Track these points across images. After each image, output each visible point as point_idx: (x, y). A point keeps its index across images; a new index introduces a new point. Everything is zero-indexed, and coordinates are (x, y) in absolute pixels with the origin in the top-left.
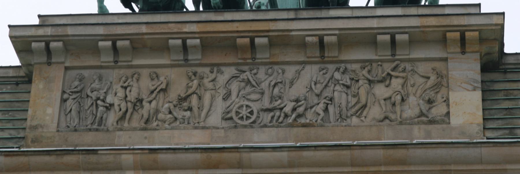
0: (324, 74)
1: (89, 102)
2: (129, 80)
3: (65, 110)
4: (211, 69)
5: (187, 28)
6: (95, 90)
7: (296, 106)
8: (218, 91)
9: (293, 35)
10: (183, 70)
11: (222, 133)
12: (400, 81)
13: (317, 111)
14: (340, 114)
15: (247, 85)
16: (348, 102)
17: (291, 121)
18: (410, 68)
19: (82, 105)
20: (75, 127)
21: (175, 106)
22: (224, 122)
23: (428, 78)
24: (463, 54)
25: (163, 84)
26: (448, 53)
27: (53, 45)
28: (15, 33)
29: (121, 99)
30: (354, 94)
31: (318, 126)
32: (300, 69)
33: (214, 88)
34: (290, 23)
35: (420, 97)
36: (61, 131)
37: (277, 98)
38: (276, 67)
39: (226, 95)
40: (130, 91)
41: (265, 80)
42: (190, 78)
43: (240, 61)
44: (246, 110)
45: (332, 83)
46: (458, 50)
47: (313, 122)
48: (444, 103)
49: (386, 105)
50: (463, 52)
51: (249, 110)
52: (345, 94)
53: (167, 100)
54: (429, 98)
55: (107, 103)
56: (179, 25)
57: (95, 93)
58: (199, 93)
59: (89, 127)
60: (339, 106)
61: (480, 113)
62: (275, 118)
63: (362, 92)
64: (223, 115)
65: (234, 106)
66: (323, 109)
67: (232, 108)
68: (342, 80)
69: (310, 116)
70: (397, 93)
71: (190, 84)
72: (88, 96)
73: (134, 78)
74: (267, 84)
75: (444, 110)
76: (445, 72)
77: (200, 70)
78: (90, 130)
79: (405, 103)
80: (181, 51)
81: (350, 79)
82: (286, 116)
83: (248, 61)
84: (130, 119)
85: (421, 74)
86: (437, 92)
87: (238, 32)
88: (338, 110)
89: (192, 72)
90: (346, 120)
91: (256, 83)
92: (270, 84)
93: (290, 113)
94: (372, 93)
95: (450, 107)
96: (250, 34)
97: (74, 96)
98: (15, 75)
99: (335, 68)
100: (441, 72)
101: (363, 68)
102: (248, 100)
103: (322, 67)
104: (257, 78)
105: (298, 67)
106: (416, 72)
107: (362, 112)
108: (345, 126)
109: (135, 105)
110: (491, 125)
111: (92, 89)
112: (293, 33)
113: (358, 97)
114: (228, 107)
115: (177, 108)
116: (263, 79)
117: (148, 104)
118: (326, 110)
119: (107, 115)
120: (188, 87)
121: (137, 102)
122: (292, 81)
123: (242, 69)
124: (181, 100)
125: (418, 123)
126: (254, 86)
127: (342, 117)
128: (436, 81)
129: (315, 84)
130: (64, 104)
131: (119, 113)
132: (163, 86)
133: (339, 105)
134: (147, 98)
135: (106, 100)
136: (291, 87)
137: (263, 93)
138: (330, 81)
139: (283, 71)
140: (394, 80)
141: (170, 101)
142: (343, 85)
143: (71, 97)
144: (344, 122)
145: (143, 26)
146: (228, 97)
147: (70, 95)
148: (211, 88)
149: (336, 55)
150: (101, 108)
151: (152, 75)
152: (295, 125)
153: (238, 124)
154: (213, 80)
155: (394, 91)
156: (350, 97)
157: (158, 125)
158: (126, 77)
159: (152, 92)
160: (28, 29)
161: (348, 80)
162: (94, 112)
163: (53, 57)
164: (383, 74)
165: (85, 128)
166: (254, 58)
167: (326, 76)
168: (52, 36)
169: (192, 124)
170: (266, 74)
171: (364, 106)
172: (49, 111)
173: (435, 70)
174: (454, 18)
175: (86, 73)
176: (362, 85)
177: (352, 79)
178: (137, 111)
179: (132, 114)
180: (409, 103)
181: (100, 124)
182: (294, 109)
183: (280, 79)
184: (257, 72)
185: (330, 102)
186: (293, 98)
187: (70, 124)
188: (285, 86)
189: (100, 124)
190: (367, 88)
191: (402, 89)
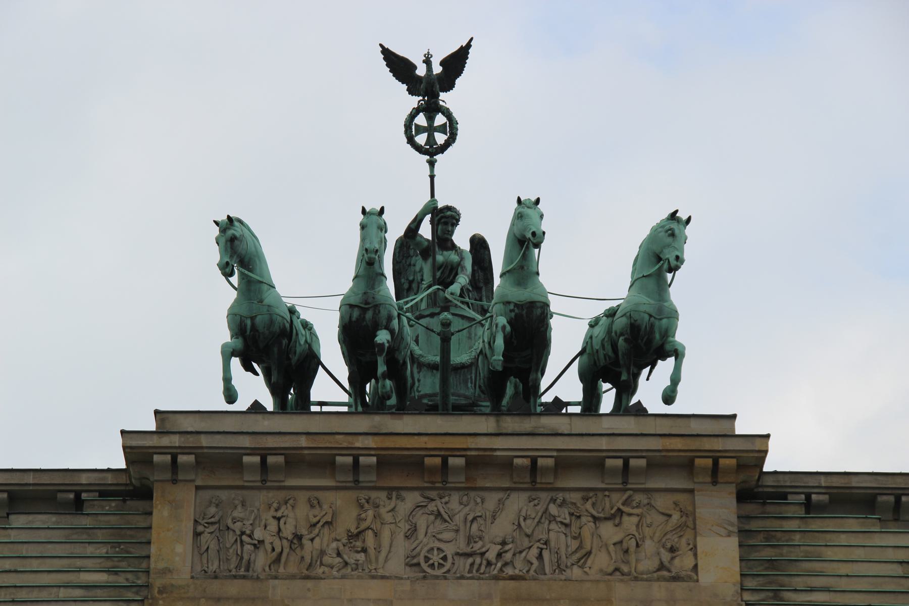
0: (535, 505)
1: (231, 538)
2: (283, 508)
3: (199, 547)
4: (389, 493)
5: (360, 442)
6: (238, 521)
7: (501, 551)
8: (399, 525)
9: (497, 456)
10: (352, 495)
11: (407, 586)
12: (635, 520)
13: (529, 558)
14: (558, 563)
15: (436, 519)
16: (567, 546)
17: (495, 572)
18: (646, 501)
19: (221, 541)
20: (215, 572)
21: (344, 546)
22: (408, 569)
23: (670, 516)
24: (715, 485)
25: (327, 515)
26: (695, 483)
27: (182, 459)
28: (131, 442)
29: (274, 534)
30: (575, 535)
31: (530, 580)
32: (505, 498)
33: (394, 521)
34: (495, 439)
35: (660, 541)
36: (197, 578)
37: (477, 539)
38: (472, 494)
39: (409, 532)
40: (285, 523)
41: (459, 512)
42: (362, 507)
43: (426, 485)
44: (438, 554)
45: (546, 518)
46: (709, 479)
47: (523, 572)
48: (689, 552)
49: (616, 552)
50: (715, 482)
51: (441, 555)
52: (563, 535)
53: (333, 535)
54: (672, 545)
55: (255, 540)
56: (350, 438)
57: (239, 524)
58: (375, 529)
59: (233, 573)
60: (557, 552)
61: (736, 567)
62: (476, 567)
63: (587, 532)
64: (407, 560)
65: (422, 548)
66: (537, 555)
67: (419, 550)
68: (559, 517)
69: (519, 563)
70: (631, 536)
71: (363, 516)
72: (228, 528)
73: (288, 505)
74: (462, 519)
75: (689, 562)
76: (690, 508)
77: (374, 495)
78: (235, 577)
79: (640, 549)
80: (350, 470)
81: (569, 513)
82: (489, 564)
83: (437, 485)
84: (286, 563)
85: (661, 511)
86: (681, 536)
87: (426, 449)
88: (555, 557)
89: (365, 499)
90: (565, 571)
91: (449, 516)
92: (466, 519)
93: (494, 561)
94: (598, 535)
95: (699, 558)
96: (442, 453)
97: (211, 529)
98: (115, 482)
99: (549, 497)
100: (686, 508)
101: (586, 499)
102: (440, 540)
103: (533, 497)
104: (449, 509)
105: (500, 495)
106: (653, 506)
107: (585, 563)
108: (565, 580)
109: (292, 542)
110: (750, 583)
111: (233, 519)
112: (498, 453)
113: (579, 539)
114: (413, 550)
115: (347, 548)
116: (457, 511)
117: (310, 542)
118: (540, 557)
119: (256, 555)
120: (360, 520)
121: (294, 538)
122: (494, 514)
123: (429, 496)
124: (352, 537)
125: (658, 579)
126: (446, 521)
127: (560, 566)
128: (680, 521)
129: (525, 519)
130: (197, 539)
131: (272, 554)
132: (328, 518)
133: (556, 550)
134: (308, 534)
135: (253, 535)
136: (493, 523)
137: (457, 531)
138: (544, 516)
139: (482, 500)
140: (625, 518)
141: (338, 538)
142: (562, 523)
143: (208, 530)
144: (562, 574)
145: (302, 437)
146: (413, 534)
147: (205, 527)
148: (390, 521)
149: (552, 481)
150: (248, 548)
151: (312, 501)
152: (501, 578)
153: (427, 574)
154: (392, 510)
155: (627, 534)
156: (569, 539)
157: (323, 573)
158: (278, 503)
159: (315, 525)
160: (148, 436)
161: (567, 516)
162: (239, 552)
163: (179, 473)
164: (612, 509)
165: (228, 574)
166: (445, 481)
167: (538, 508)
168: (180, 447)
169: (367, 571)
170: (461, 503)
171: (589, 553)
172: (179, 549)
173: (679, 505)
174: (705, 439)
175: (224, 495)
176: (586, 524)
177: (571, 514)
178: (294, 551)
179: (288, 555)
180: (645, 550)
181: (247, 570)
182: (499, 555)
183: (479, 512)
184: (449, 501)
185: (545, 547)
186: (499, 540)
187: (208, 568)
188: (485, 520)
189: (247, 570)
190: (591, 527)
191: (637, 531)
